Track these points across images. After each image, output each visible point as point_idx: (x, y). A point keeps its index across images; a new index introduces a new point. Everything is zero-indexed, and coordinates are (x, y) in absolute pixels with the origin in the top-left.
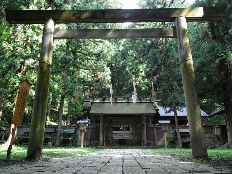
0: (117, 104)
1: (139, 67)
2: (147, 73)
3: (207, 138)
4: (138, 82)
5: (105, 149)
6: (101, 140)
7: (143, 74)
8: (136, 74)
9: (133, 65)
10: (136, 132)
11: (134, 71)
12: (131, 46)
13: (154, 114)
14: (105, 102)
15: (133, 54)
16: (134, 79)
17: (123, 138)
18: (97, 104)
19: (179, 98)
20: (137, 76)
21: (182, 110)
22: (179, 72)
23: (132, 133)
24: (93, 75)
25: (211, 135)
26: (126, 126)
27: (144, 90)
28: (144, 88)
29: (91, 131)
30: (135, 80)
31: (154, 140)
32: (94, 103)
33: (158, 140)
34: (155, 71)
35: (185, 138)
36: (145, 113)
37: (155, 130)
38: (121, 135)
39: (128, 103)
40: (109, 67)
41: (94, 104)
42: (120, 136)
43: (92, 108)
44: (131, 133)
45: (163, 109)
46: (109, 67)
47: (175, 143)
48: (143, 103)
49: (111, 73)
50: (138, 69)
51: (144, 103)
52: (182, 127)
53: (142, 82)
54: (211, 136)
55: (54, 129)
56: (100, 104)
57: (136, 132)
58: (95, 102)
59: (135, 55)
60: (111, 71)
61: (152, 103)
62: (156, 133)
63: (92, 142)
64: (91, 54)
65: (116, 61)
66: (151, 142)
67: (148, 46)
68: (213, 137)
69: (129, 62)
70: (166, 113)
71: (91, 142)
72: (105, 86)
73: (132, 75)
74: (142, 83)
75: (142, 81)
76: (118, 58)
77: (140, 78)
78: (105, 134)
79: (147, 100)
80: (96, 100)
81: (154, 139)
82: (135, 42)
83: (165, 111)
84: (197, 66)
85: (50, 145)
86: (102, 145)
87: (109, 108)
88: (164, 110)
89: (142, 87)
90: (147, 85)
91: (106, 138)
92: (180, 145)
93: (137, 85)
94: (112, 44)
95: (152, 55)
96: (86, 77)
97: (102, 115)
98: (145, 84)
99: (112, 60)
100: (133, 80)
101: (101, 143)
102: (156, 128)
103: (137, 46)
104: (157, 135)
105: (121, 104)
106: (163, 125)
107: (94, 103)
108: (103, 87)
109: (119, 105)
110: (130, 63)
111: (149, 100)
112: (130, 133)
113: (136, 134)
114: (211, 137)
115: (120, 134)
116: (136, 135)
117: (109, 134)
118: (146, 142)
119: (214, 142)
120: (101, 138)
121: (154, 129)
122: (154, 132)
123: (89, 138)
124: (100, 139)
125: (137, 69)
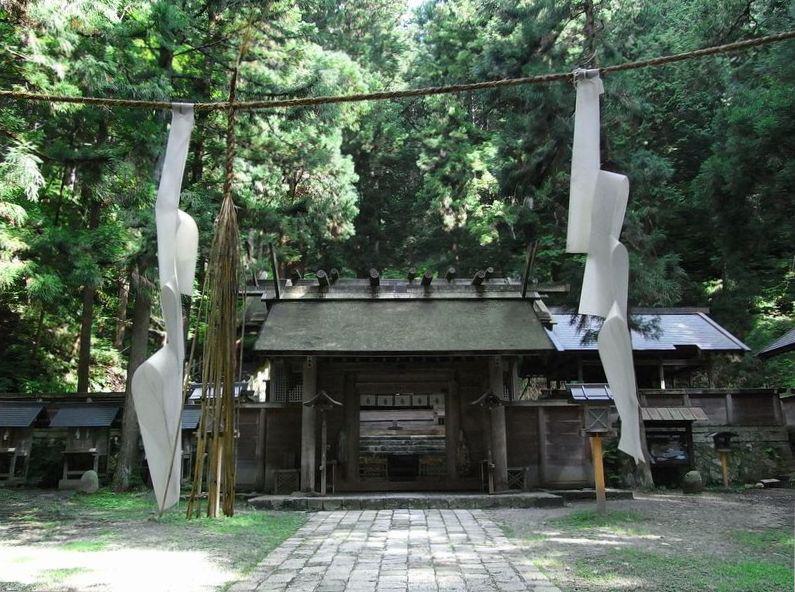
0: (380, 305)
1: (470, 156)
2: (504, 176)
3: (749, 445)
4: (465, 216)
5: (323, 509)
6: (308, 466)
7: (488, 180)
8: (457, 182)
9: (445, 149)
10: (460, 428)
11: (447, 169)
12: (438, 76)
13: (544, 351)
14: (327, 296)
15: (444, 104)
16: (448, 201)
17: (403, 442)
18: (292, 307)
19: (651, 281)
20: (460, 191)
21: (654, 331)
22: (646, 166)
23: (441, 421)
24: (286, 187)
25: (767, 429)
26: (416, 398)
27: (488, 245)
28: (487, 239)
29: (266, 421)
30: (450, 206)
31: (539, 462)
32: (277, 300)
33: (559, 461)
34: (539, 165)
35: (663, 447)
36: (504, 346)
37: (544, 419)
39: (427, 300)
40: (350, 157)
41: (279, 306)
42: (394, 432)
43: (268, 323)
44: (436, 420)
45: (574, 327)
46: (350, 157)
47: (622, 466)
48: (492, 303)
49: (357, 178)
50: (465, 165)
51: (496, 304)
52: (648, 397)
53: (481, 214)
54: (765, 434)
55: (114, 412)
56: (303, 304)
57: (460, 428)
58: (281, 297)
59: (452, 110)
60: (357, 170)
61: (532, 301)
62: (544, 431)
63: (270, 472)
64: (269, 91)
65: (378, 132)
66: (525, 470)
67: (511, 56)
68: (772, 438)
69: (430, 136)
70: (585, 341)
71: (267, 470)
72: (334, 231)
73: (441, 190)
74: (479, 219)
75: (479, 212)
76: (388, 121)
77: (471, 200)
78: (324, 441)
79: (506, 289)
80: (288, 289)
81: (536, 456)
82: (452, 59)
83: (583, 334)
84: (768, 128)
85: (89, 482)
86: (312, 486)
87: (343, 325)
88: (579, 328)
89: (479, 233)
90: (501, 226)
91: (331, 455)
92: (644, 477)
93: (460, 225)
94: (363, 66)
95: (535, 91)
96: (261, 196)
97: (309, 358)
98: (490, 221)
99: (362, 127)
100: (444, 206)
101: (308, 479)
102: (548, 409)
103: (459, 75)
104: (549, 437)
105: (401, 308)
106: (587, 408)
107: (277, 300)
108: (328, 235)
109: (390, 309)
110: (434, 142)
111: (515, 289)
112: (432, 420)
113: (462, 433)
114: (765, 438)
115: (391, 425)
116: (461, 438)
117: (343, 437)
118: (505, 475)
119: (779, 460)
120: (308, 459)
121: (538, 411)
122: (538, 428)
123: (258, 452)
124: (303, 462)
125: (459, 166)
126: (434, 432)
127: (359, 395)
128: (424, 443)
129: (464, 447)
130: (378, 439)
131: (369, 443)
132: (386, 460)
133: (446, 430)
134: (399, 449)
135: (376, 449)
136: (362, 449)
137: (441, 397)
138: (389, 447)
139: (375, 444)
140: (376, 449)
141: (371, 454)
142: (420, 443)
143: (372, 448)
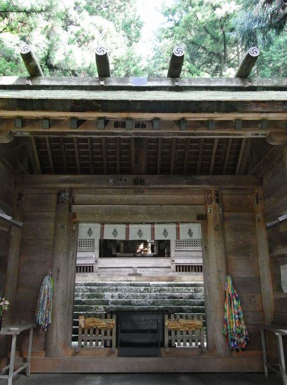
10: (228, 273)
17: (142, 288)
38: (135, 274)
42: (133, 278)
44: (173, 268)
57: (228, 273)
113: (230, 282)
115: (131, 271)
116: (230, 289)
117: (48, 284)
126: (171, 279)
127: (77, 223)
128: (164, 290)
129: (235, 302)
130: (116, 285)
131: (105, 290)
132: (113, 321)
133: (204, 278)
135: (112, 297)
136: (97, 297)
137: (196, 228)
138: (127, 295)
139: (112, 290)
141: (106, 303)
142: (160, 291)
143: (108, 296)
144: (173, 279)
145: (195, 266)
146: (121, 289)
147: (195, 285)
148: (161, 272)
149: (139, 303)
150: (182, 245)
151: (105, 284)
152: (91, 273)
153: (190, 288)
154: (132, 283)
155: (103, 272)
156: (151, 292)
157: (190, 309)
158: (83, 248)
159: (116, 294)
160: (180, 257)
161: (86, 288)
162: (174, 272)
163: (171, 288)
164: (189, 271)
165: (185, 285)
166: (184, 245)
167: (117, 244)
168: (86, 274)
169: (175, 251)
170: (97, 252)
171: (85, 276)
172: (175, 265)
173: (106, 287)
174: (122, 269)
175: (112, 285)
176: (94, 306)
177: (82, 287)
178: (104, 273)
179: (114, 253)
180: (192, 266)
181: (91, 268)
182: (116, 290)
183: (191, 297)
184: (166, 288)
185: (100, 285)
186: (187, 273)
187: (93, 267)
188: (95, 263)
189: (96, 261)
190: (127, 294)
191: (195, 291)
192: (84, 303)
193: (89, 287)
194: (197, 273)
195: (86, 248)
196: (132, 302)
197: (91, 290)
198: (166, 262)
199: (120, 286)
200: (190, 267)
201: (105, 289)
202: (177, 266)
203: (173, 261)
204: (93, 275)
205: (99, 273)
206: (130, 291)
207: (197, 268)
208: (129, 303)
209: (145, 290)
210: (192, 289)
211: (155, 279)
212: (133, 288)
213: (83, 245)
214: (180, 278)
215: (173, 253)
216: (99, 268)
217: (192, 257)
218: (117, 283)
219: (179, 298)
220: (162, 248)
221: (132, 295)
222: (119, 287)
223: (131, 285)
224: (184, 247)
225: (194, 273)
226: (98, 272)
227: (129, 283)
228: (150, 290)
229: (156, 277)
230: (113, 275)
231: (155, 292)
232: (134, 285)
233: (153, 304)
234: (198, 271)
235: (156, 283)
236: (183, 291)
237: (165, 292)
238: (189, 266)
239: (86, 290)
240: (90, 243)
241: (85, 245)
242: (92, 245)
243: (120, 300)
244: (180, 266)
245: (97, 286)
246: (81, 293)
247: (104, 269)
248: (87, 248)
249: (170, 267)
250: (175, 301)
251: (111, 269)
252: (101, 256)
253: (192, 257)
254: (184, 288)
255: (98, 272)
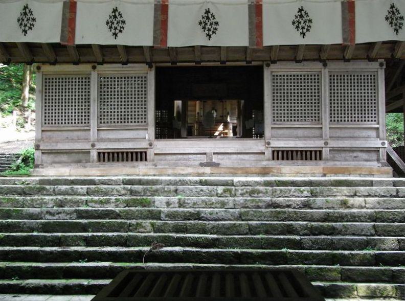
17: (220, 189)
38: (210, 164)
42: (207, 170)
44: (268, 154)
115: (204, 159)
126: (265, 172)
128: (259, 192)
130: (176, 183)
131: (155, 193)
134: (211, 205)
136: (143, 204)
138: (195, 200)
140: (168, 204)
141: (156, 215)
142: (251, 193)
143: (160, 202)
144: (267, 170)
145: (302, 152)
146: (183, 191)
147: (310, 184)
148: (249, 161)
149: (215, 216)
150: (283, 119)
151: (157, 180)
152: (144, 162)
153: (303, 188)
154: (203, 178)
155: (161, 160)
156: (235, 195)
157: (306, 228)
158: (130, 124)
159: (174, 199)
160: (278, 138)
161: (124, 188)
162: (269, 160)
163: (270, 188)
164: (292, 159)
165: (293, 184)
166: (286, 119)
167: (189, 125)
168: (135, 163)
169: (272, 128)
170: (151, 131)
171: (134, 167)
172: (270, 150)
173: (158, 187)
174: (190, 156)
175: (170, 183)
176: (134, 222)
177: (117, 187)
178: (163, 162)
179: (184, 133)
180: (297, 152)
181: (144, 154)
182: (176, 191)
183: (306, 205)
184: (261, 188)
185: (148, 183)
186: (290, 162)
187: (146, 153)
188: (148, 147)
189: (151, 145)
190: (195, 199)
191: (313, 194)
192: (118, 216)
193: (129, 187)
194: (304, 162)
195: (135, 124)
196: (203, 215)
197: (132, 192)
198: (257, 145)
199: (183, 185)
200: (294, 154)
201: (157, 191)
202: (273, 152)
203: (269, 143)
204: (146, 165)
205: (155, 162)
206: (199, 193)
207: (304, 153)
208: (197, 216)
209: (225, 191)
210: (306, 190)
211: (240, 172)
212: (204, 188)
213: (130, 120)
214: (279, 168)
215: (268, 132)
216: (155, 154)
217: (298, 138)
218: (178, 178)
219: (284, 207)
220: (249, 128)
221: (203, 201)
222: (180, 188)
223: (202, 183)
224: (286, 122)
225: (300, 162)
226: (153, 161)
227: (197, 178)
228: (233, 193)
229: (242, 168)
230: (176, 165)
231: (242, 195)
232: (206, 183)
233: (240, 217)
234: (306, 159)
235: (243, 179)
236: (292, 193)
237: (261, 195)
238: (292, 152)
239: (123, 192)
240: (140, 117)
241: (133, 120)
242: (143, 120)
243: (182, 209)
244: (278, 152)
245: (143, 184)
246: (113, 198)
247: (162, 157)
248: (137, 124)
249: (264, 153)
250: (279, 213)
251: (174, 157)
252: (156, 138)
253: (298, 137)
254: (293, 188)
255: (153, 161)
